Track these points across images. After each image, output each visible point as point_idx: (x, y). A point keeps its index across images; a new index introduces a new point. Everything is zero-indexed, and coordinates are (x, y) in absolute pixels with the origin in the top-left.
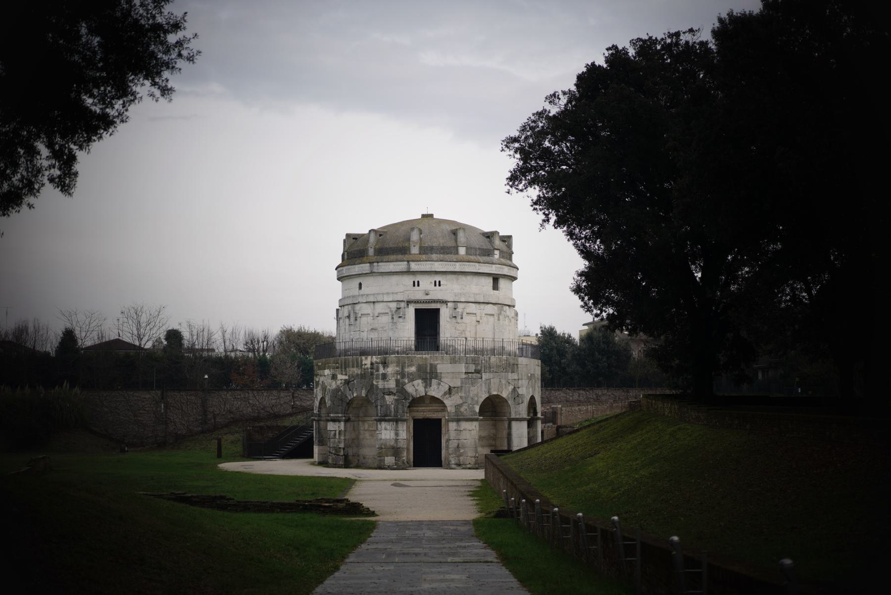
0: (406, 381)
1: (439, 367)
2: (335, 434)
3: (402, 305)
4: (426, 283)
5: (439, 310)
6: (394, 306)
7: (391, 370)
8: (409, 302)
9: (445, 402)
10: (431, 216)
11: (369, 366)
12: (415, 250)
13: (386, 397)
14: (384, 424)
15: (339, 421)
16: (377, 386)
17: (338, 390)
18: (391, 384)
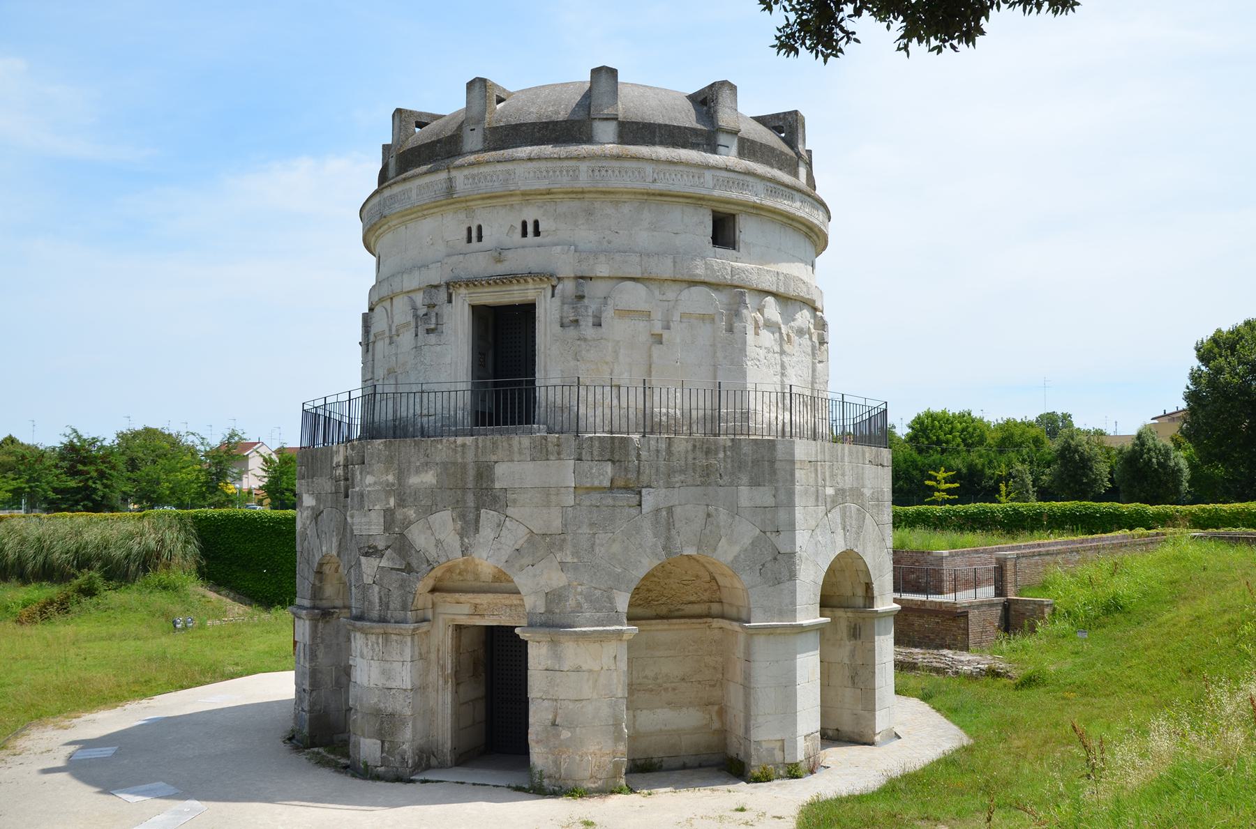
0: (411, 513)
1: (500, 470)
12: (473, 140)
13: (363, 559)
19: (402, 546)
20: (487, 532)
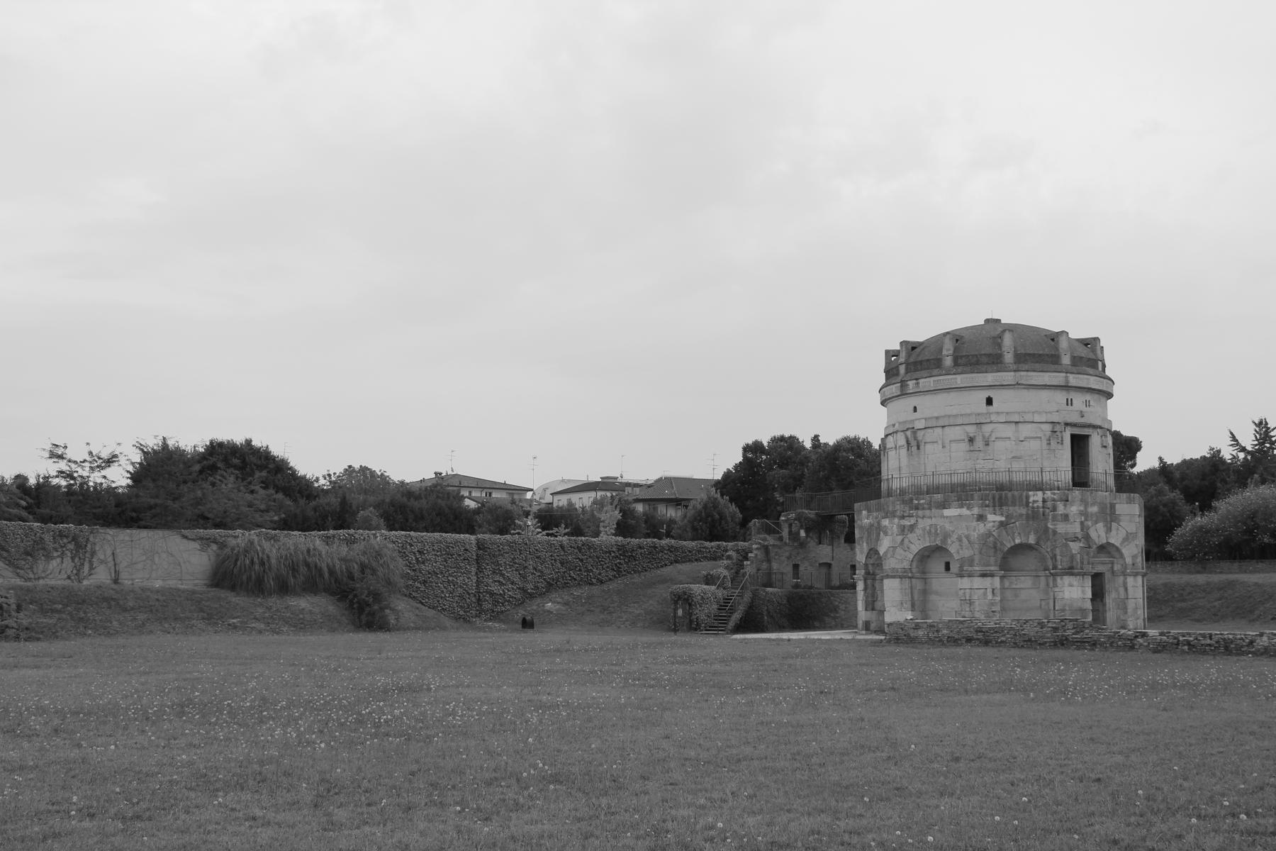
2: (985, 594)
3: (1058, 428)
4: (1079, 400)
5: (1087, 437)
6: (1048, 428)
7: (1074, 509)
8: (1067, 424)
9: (1124, 551)
10: (998, 321)
11: (1040, 504)
14: (1067, 579)
15: (992, 576)
16: (1055, 532)
17: (989, 534)
18: (1075, 528)
19: (1087, 537)
20: (1114, 532)
